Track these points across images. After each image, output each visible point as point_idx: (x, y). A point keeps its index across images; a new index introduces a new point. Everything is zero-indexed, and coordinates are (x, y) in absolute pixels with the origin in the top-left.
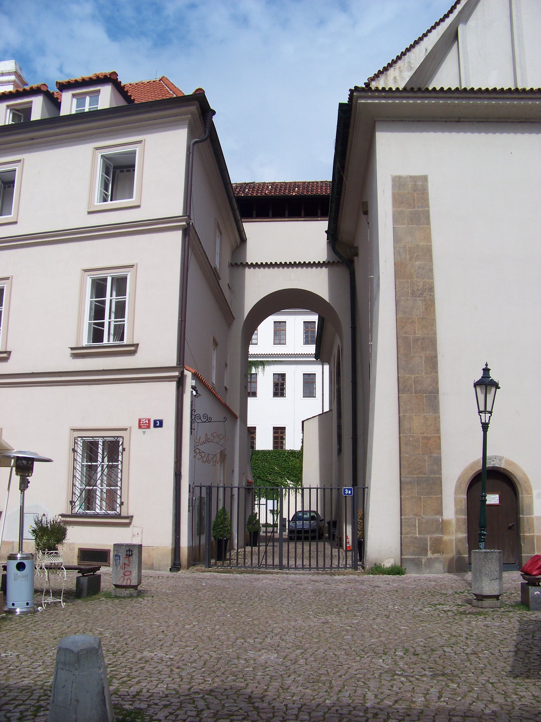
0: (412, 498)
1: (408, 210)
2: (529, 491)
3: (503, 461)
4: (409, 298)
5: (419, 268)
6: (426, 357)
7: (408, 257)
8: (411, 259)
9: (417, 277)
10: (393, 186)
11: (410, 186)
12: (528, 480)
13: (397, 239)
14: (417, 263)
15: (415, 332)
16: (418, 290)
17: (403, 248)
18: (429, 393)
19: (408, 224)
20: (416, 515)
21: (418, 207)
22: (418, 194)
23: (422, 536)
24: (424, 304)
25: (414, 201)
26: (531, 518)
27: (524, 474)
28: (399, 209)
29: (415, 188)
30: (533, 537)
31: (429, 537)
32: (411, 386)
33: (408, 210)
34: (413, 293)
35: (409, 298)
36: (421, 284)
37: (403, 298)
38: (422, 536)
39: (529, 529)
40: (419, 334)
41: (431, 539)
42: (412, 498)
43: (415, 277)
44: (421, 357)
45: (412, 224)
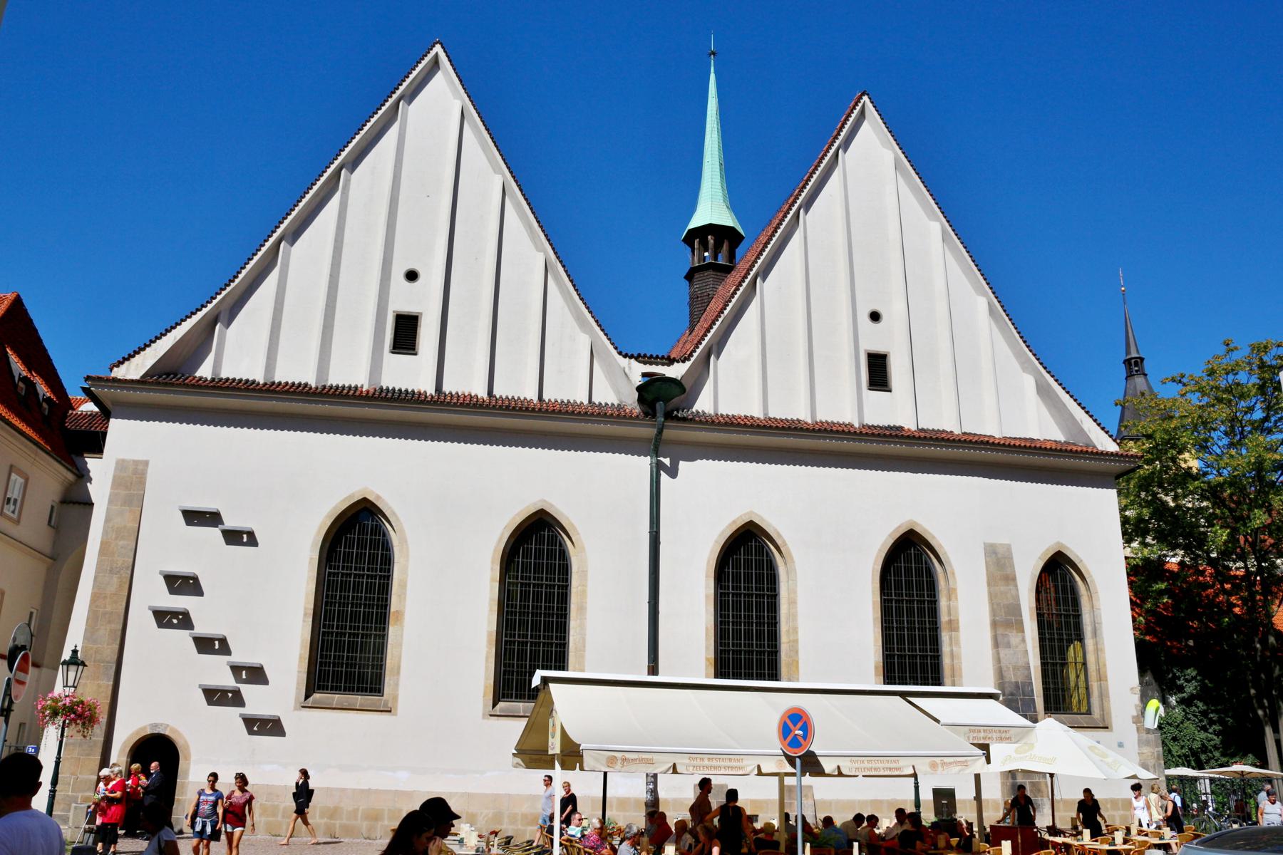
0: (72, 758)
1: (124, 492)
2: (188, 758)
3: (168, 729)
4: (107, 575)
5: (122, 547)
6: (111, 630)
7: (114, 536)
8: (116, 539)
9: (118, 556)
10: (116, 469)
11: (131, 469)
12: (188, 746)
13: (107, 520)
14: (121, 543)
15: (105, 607)
16: (117, 568)
17: (112, 528)
18: (108, 662)
19: (121, 506)
20: (72, 774)
21: (134, 490)
22: (136, 477)
23: (74, 794)
24: (119, 580)
25: (131, 483)
26: (184, 782)
27: (186, 742)
28: (116, 491)
29: (135, 472)
30: (185, 799)
31: (80, 795)
32: (91, 656)
33: (124, 492)
34: (111, 571)
35: (107, 575)
36: (120, 563)
37: (101, 574)
38: (74, 794)
39: (182, 793)
40: (109, 609)
41: (82, 797)
42: (72, 758)
43: (116, 555)
44: (106, 629)
45: (125, 506)
